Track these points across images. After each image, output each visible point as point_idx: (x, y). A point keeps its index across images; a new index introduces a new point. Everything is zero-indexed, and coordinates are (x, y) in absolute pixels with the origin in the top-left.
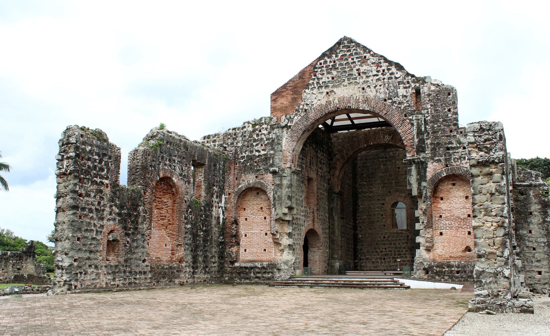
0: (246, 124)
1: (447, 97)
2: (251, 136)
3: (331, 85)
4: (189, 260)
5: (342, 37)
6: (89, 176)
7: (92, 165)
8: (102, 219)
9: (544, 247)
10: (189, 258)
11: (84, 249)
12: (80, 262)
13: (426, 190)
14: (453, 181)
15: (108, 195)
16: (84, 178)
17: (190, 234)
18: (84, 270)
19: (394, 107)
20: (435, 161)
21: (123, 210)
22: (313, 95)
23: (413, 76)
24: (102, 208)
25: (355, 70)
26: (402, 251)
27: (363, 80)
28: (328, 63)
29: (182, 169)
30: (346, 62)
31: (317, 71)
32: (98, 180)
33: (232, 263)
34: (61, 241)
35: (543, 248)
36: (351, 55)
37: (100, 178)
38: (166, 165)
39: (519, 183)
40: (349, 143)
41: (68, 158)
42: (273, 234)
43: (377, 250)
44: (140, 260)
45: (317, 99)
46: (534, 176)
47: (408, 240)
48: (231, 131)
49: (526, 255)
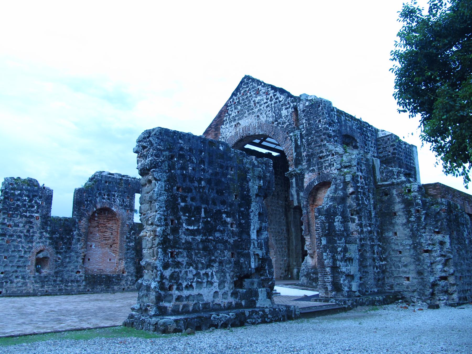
1: (318, 110)
3: (237, 118)
4: (131, 271)
5: (244, 76)
6: (19, 212)
7: (21, 204)
8: (32, 242)
9: (409, 250)
10: (132, 269)
11: (11, 265)
12: (7, 274)
13: (303, 200)
15: (39, 225)
16: (13, 214)
17: (133, 250)
18: (10, 280)
19: (279, 128)
20: (310, 171)
21: (54, 235)
22: (227, 129)
24: (31, 234)
27: (258, 109)
29: (123, 200)
30: (246, 97)
31: (229, 109)
32: (28, 214)
35: (408, 251)
36: (249, 90)
37: (29, 213)
38: (104, 199)
39: (381, 183)
44: (72, 271)
45: (229, 132)
46: (396, 174)
49: (392, 260)
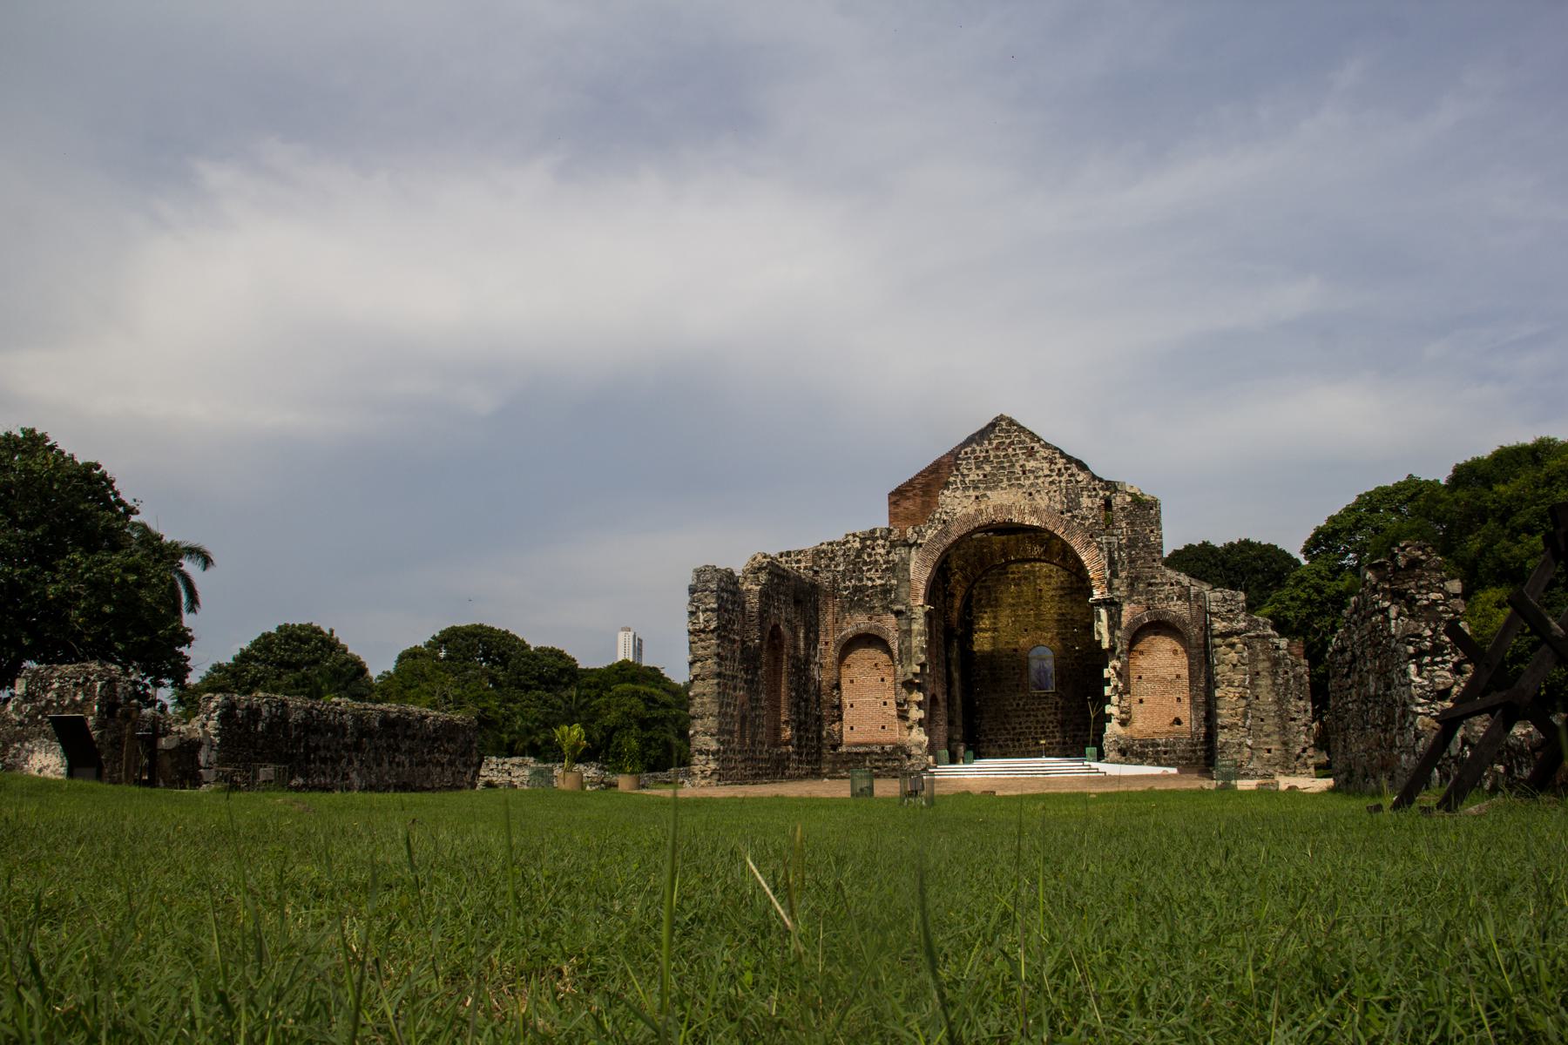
0: (850, 538)
1: (1149, 513)
2: (857, 557)
14: (1157, 628)
20: (1133, 601)
23: (1101, 480)
25: (1017, 465)
26: (1048, 728)
28: (978, 453)
33: (834, 747)
34: (701, 719)
36: (1012, 443)
40: (975, 555)
41: (707, 610)
42: (899, 704)
43: (1007, 726)
47: (1056, 708)
48: (824, 547)
